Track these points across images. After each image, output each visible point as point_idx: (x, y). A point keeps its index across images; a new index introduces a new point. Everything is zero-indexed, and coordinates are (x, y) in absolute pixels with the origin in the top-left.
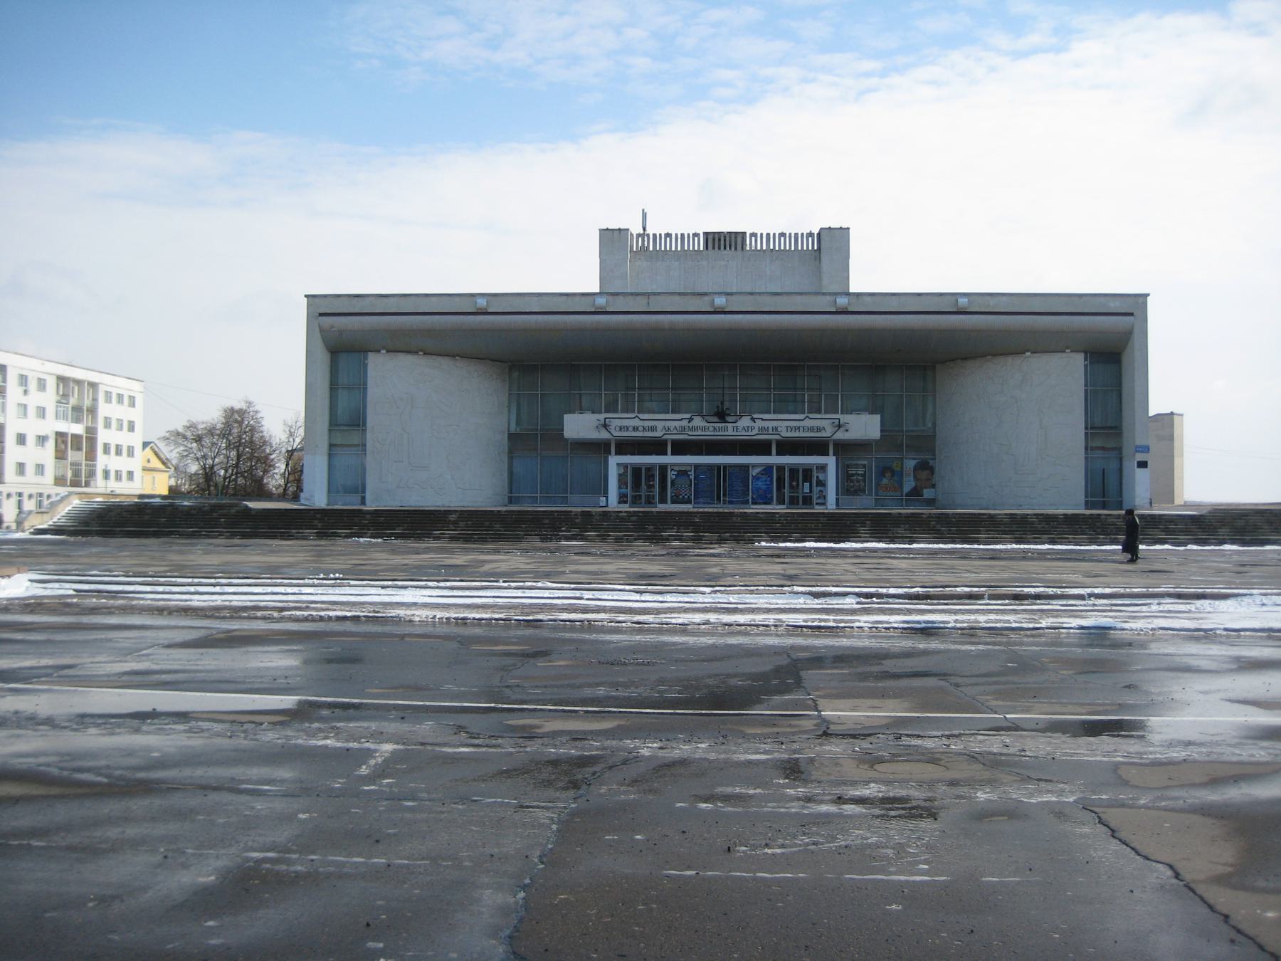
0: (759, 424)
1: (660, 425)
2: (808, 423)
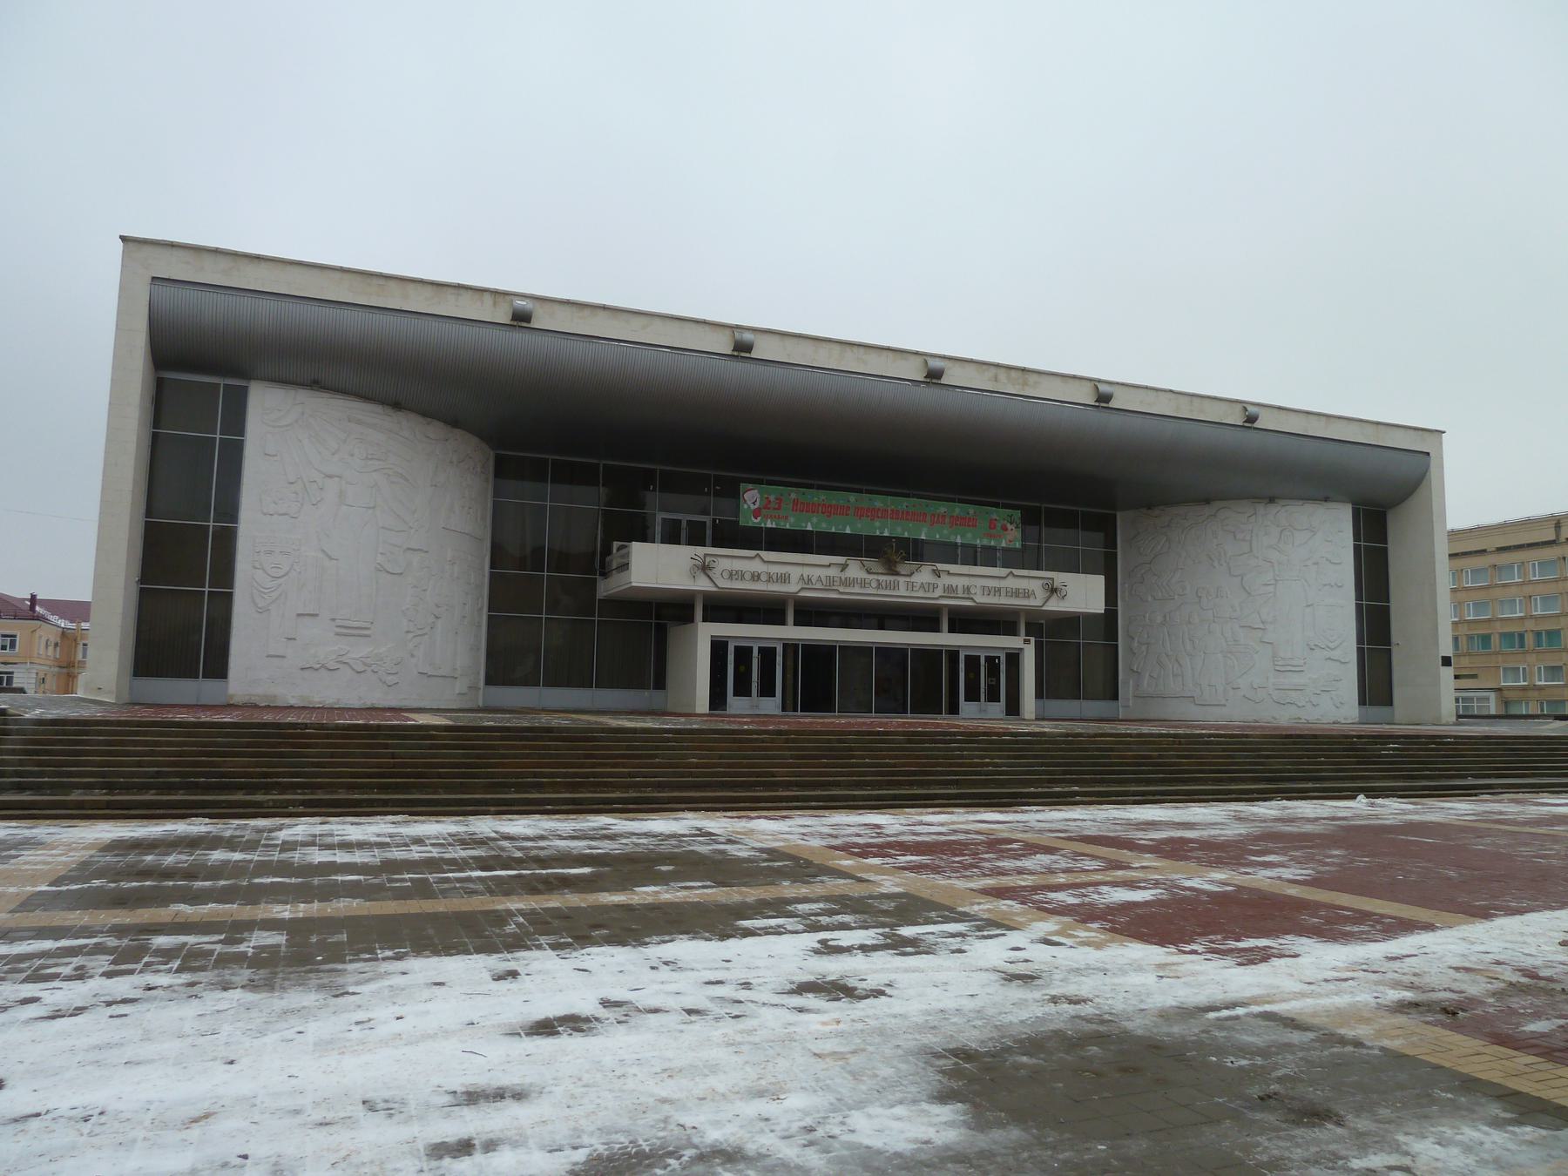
0: (946, 580)
1: (795, 573)
2: (1011, 583)
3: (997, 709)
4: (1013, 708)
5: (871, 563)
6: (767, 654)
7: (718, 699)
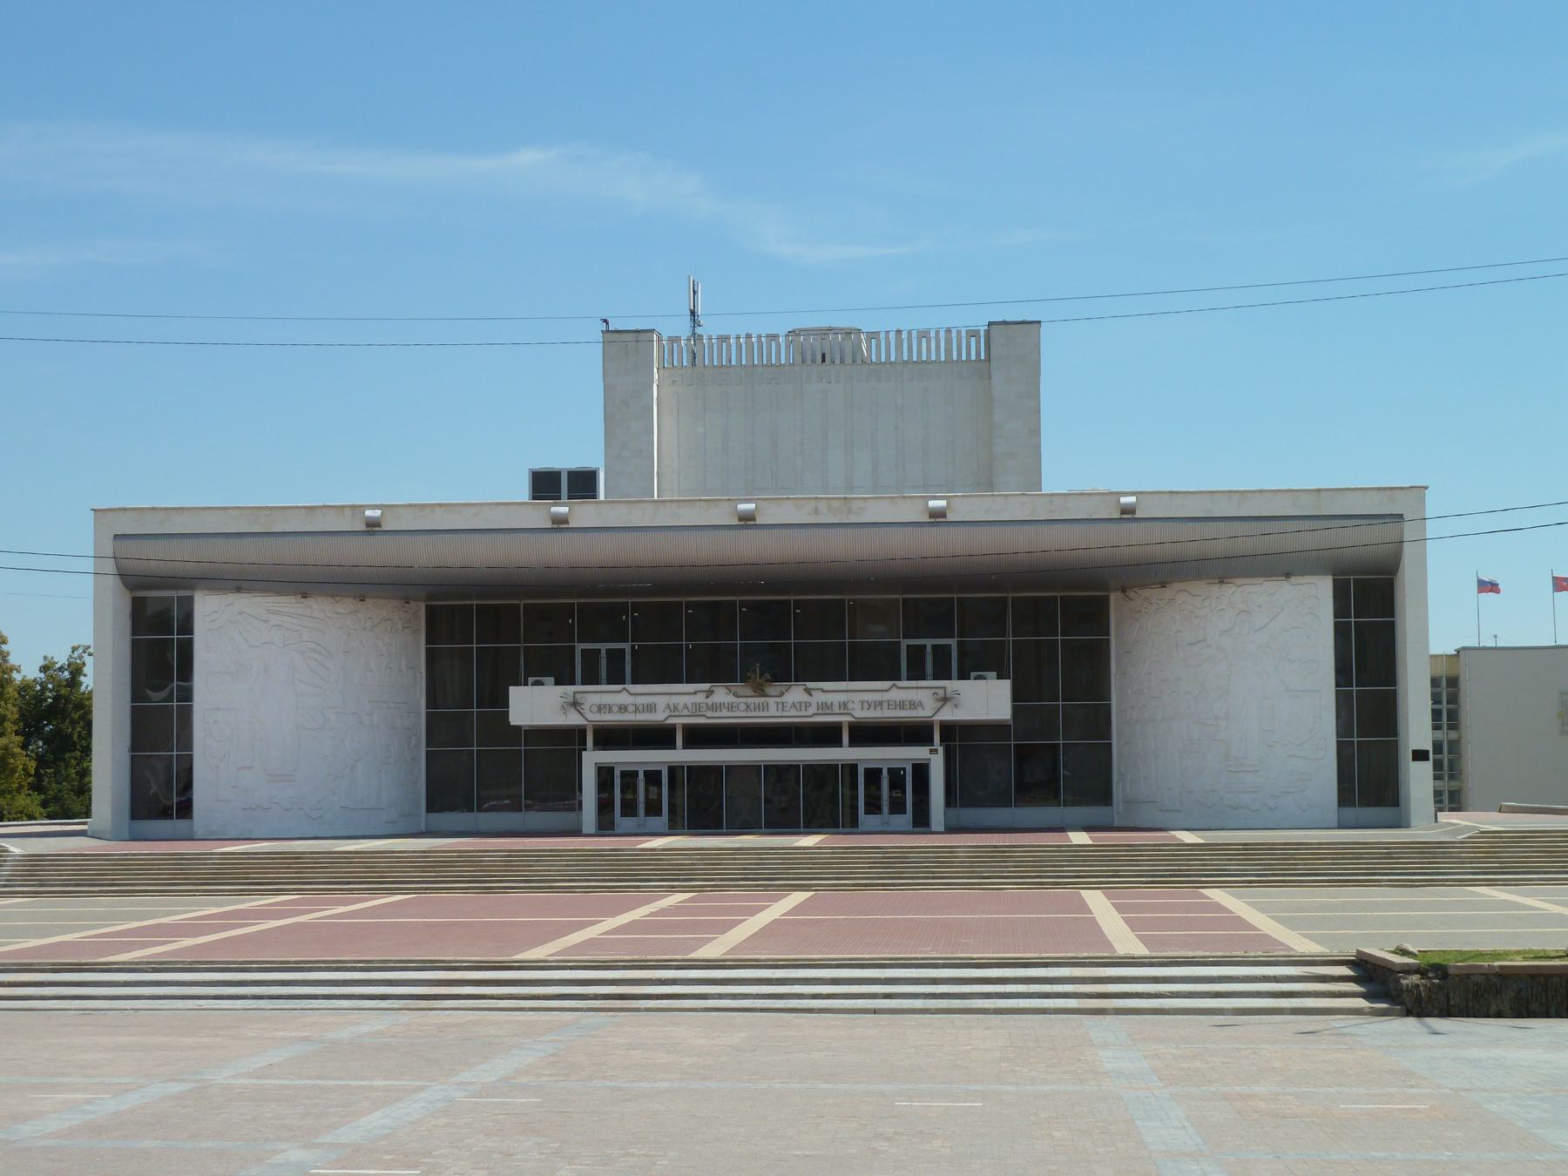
0: (819, 697)
1: (661, 702)
5: (738, 686)
6: (653, 777)
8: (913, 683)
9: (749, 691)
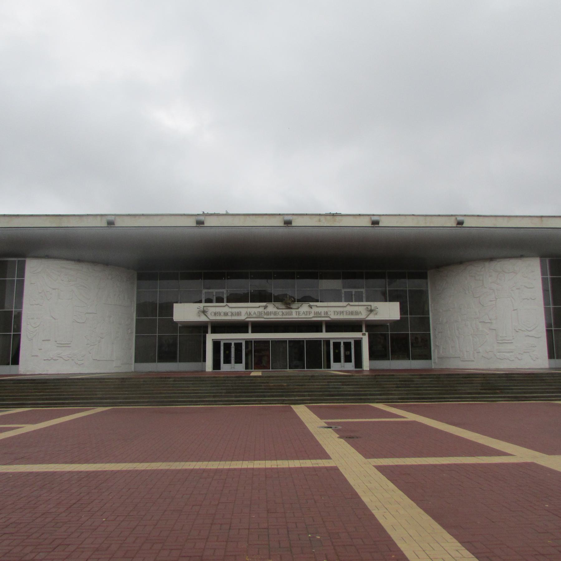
0: (315, 309)
1: (243, 311)
2: (349, 309)
3: (350, 366)
4: (359, 364)
5: (278, 304)
6: (238, 346)
7: (217, 365)
8: (357, 303)
9: (284, 307)
